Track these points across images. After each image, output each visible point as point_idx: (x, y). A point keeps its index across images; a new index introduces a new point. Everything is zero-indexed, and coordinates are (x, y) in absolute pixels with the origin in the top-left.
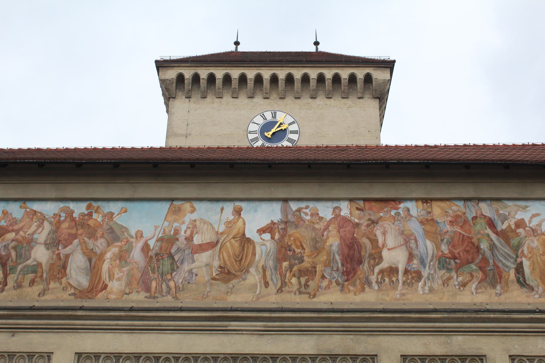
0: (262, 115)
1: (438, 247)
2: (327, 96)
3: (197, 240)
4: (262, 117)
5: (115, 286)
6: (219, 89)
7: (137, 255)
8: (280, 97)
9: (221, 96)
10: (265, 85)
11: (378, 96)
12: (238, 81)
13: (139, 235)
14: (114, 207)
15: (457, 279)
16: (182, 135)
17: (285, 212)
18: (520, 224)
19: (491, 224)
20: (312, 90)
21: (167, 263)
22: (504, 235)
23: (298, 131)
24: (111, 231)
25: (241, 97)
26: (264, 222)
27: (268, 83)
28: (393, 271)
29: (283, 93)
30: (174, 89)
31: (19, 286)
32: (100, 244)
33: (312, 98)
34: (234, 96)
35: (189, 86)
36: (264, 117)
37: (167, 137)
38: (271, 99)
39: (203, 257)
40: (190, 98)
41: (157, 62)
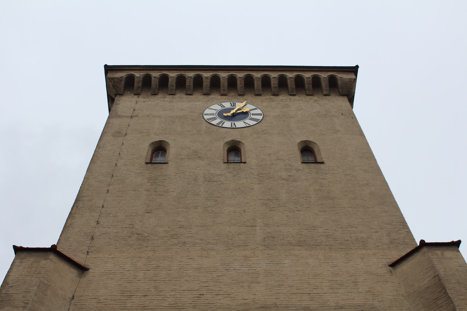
0: (219, 105)
2: (291, 94)
4: (220, 106)
6: (171, 86)
8: (239, 94)
9: (174, 93)
10: (222, 82)
11: (346, 93)
12: (193, 80)
16: (127, 117)
20: (274, 88)
23: (261, 114)
25: (196, 95)
27: (226, 81)
29: (242, 90)
30: (122, 87)
33: (273, 95)
34: (188, 93)
35: (139, 84)
36: (221, 105)
37: (108, 118)
38: (229, 96)
40: (140, 95)
41: (106, 66)
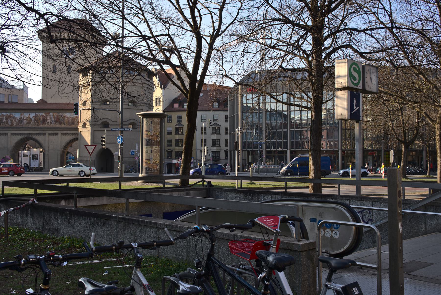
1: (54, 119)
3: (24, 118)
5: (15, 125)
7: (17, 120)
13: (17, 118)
14: (13, 114)
15: (56, 123)
17: (35, 114)
18: (65, 116)
19: (61, 116)
21: (21, 122)
22: (63, 118)
24: (13, 117)
26: (33, 116)
28: (49, 122)
31: (2, 125)
32: (12, 119)
39: (25, 121)
